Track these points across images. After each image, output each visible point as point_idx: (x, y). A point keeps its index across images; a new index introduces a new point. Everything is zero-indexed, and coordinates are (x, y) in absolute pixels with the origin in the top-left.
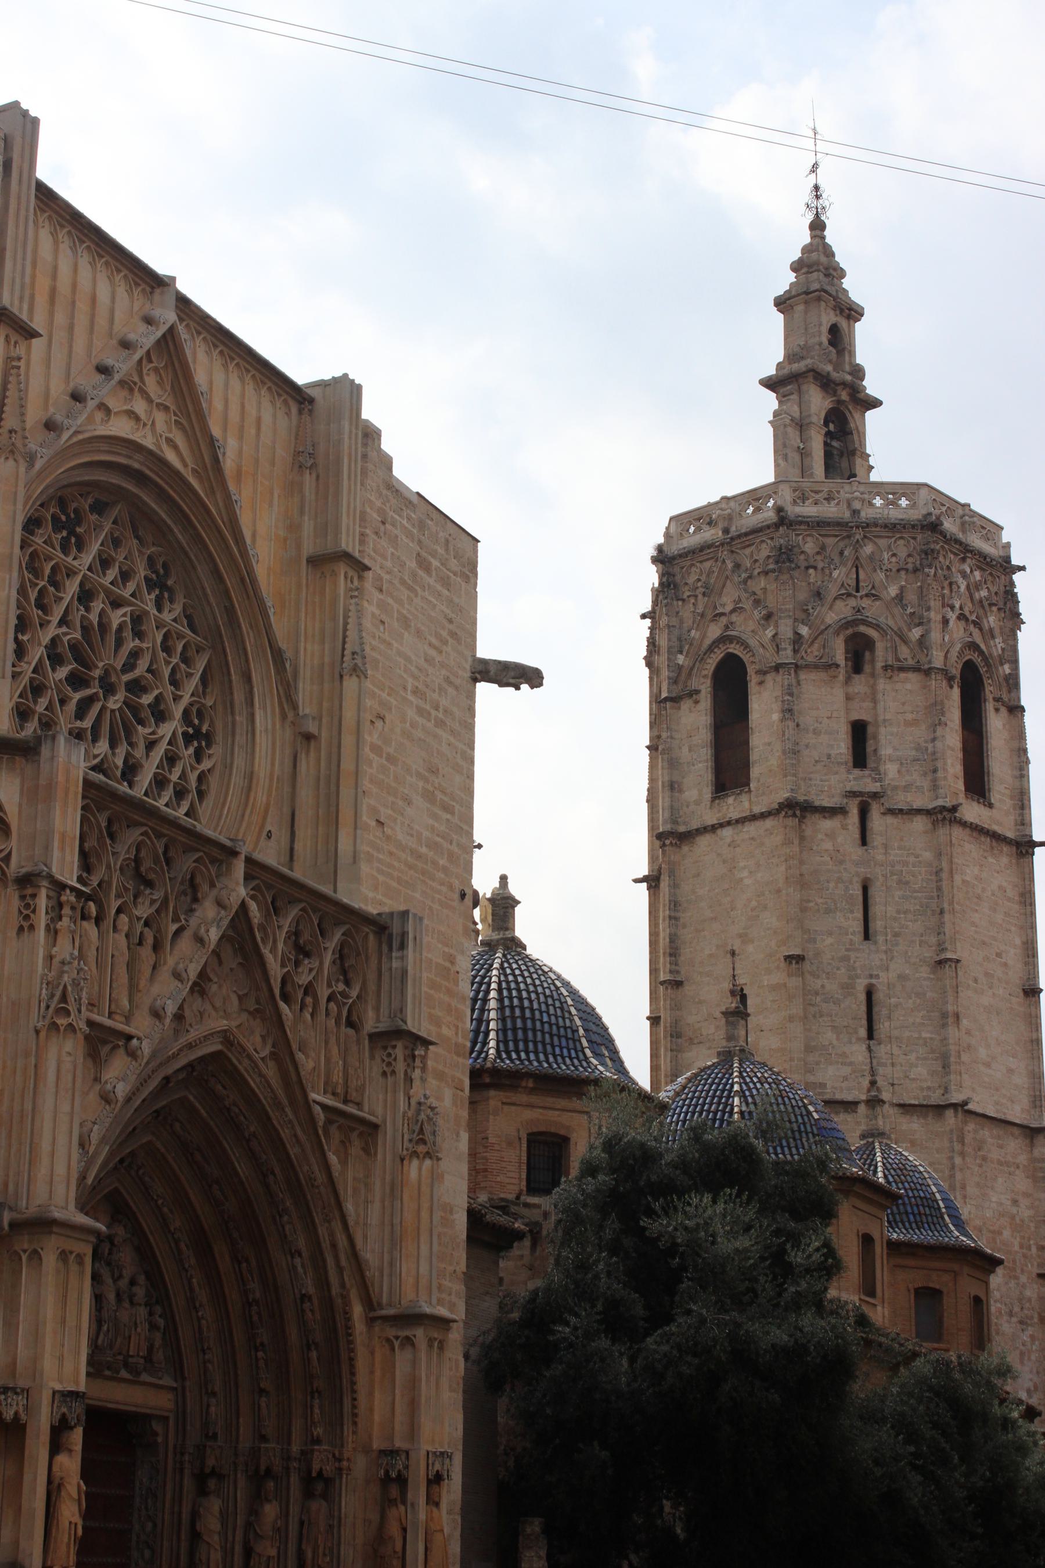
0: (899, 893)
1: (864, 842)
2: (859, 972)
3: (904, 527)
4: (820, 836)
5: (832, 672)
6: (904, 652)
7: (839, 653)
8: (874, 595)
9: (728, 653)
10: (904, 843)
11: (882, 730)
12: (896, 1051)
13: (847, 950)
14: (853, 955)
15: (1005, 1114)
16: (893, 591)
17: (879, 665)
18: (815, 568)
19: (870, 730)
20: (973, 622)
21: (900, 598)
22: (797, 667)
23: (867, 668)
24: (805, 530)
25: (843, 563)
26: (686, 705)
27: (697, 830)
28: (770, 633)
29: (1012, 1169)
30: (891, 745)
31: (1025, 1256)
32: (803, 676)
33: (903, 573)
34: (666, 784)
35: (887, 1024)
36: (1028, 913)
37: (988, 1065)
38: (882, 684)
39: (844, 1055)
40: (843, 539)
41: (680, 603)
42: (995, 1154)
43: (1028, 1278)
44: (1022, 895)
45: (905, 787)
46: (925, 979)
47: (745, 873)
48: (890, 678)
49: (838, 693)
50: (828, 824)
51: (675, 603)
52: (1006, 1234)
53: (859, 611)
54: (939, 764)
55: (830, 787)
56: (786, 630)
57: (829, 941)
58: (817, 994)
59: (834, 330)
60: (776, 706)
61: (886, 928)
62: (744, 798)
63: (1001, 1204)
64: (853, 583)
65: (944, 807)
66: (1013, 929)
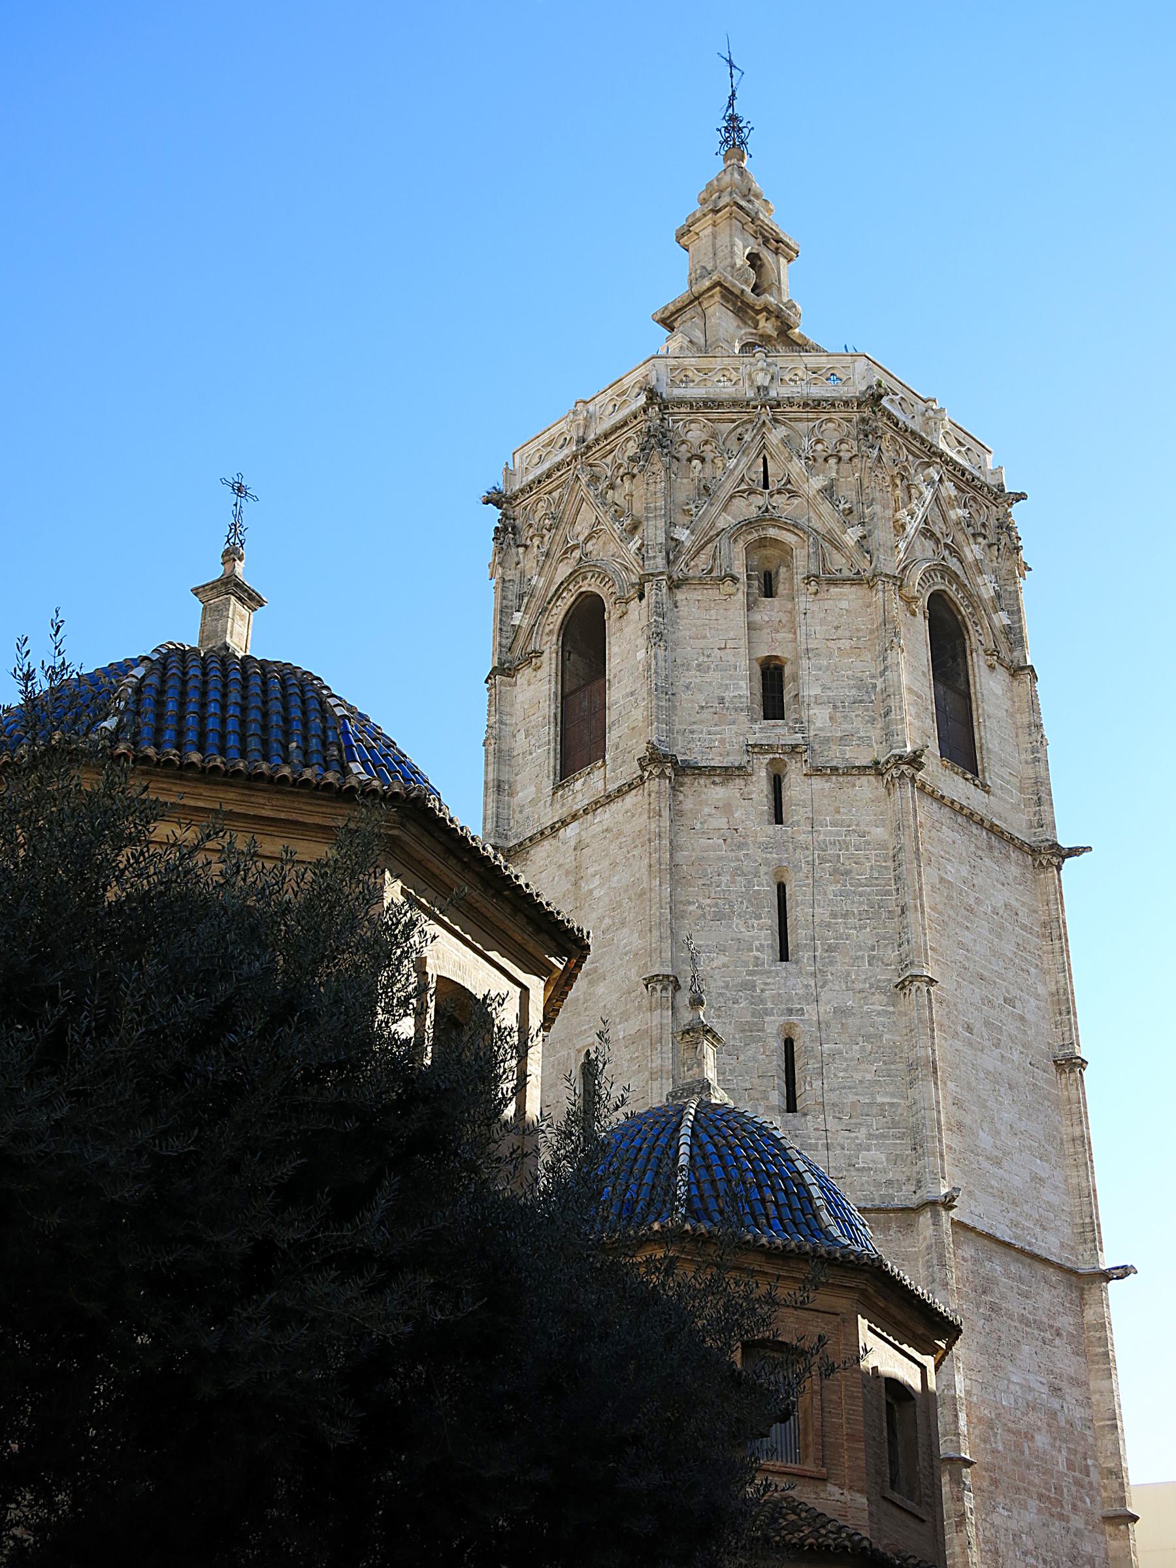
1: (779, 819)
3: (833, 405)
4: (706, 810)
5: (728, 587)
6: (838, 561)
9: (582, 593)
10: (843, 817)
11: (804, 663)
12: (832, 1124)
14: (759, 980)
15: (1030, 1244)
16: (817, 482)
17: (798, 579)
18: (703, 460)
19: (787, 671)
20: (946, 546)
21: (829, 491)
22: (675, 585)
23: (782, 588)
25: (744, 452)
27: (531, 839)
28: (634, 545)
29: (1048, 1335)
31: (1078, 1483)
32: (680, 595)
33: (832, 461)
34: (491, 785)
35: (817, 1084)
36: (1057, 949)
37: (998, 1163)
41: (521, 550)
42: (1013, 1304)
43: (1087, 1523)
44: (1044, 925)
45: (841, 738)
46: (879, 1014)
47: (597, 881)
48: (816, 593)
50: (718, 793)
51: (514, 550)
52: (1042, 1440)
53: (767, 510)
54: (892, 703)
56: (654, 531)
57: (722, 959)
59: (754, 259)
60: (642, 641)
62: (598, 774)
63: (1031, 1389)
65: (901, 757)
66: (1033, 970)
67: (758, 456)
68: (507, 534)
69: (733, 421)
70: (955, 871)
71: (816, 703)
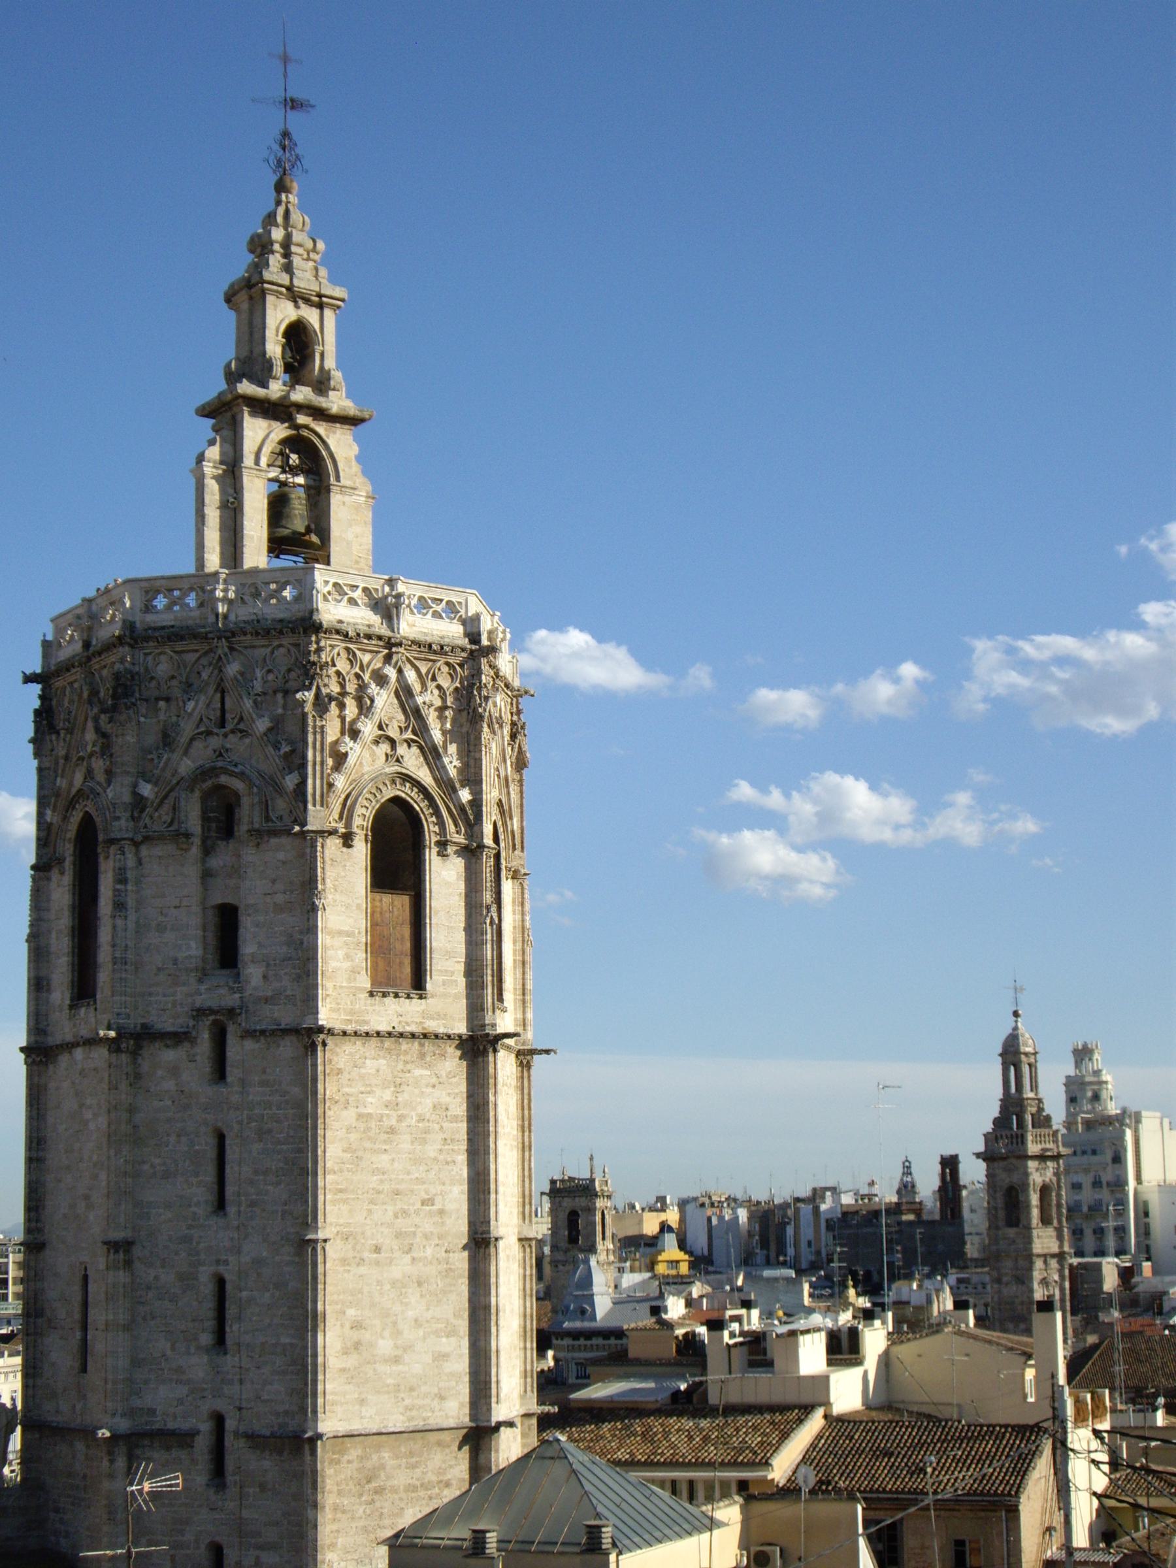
0: (256, 1147)
2: (203, 1257)
3: (281, 632)
8: (241, 731)
13: (190, 1227)
16: (262, 725)
18: (167, 700)
24: (156, 647)
26: (55, 874)
32: (144, 851)
39: (179, 1370)
40: (206, 653)
41: (54, 737)
49: (192, 872)
50: (170, 1056)
51: (48, 738)
53: (221, 755)
55: (174, 1004)
57: (169, 1215)
58: (149, 1288)
61: (239, 1195)
64: (215, 715)
67: (216, 691)
68: (45, 718)
69: (197, 651)
71: (253, 961)
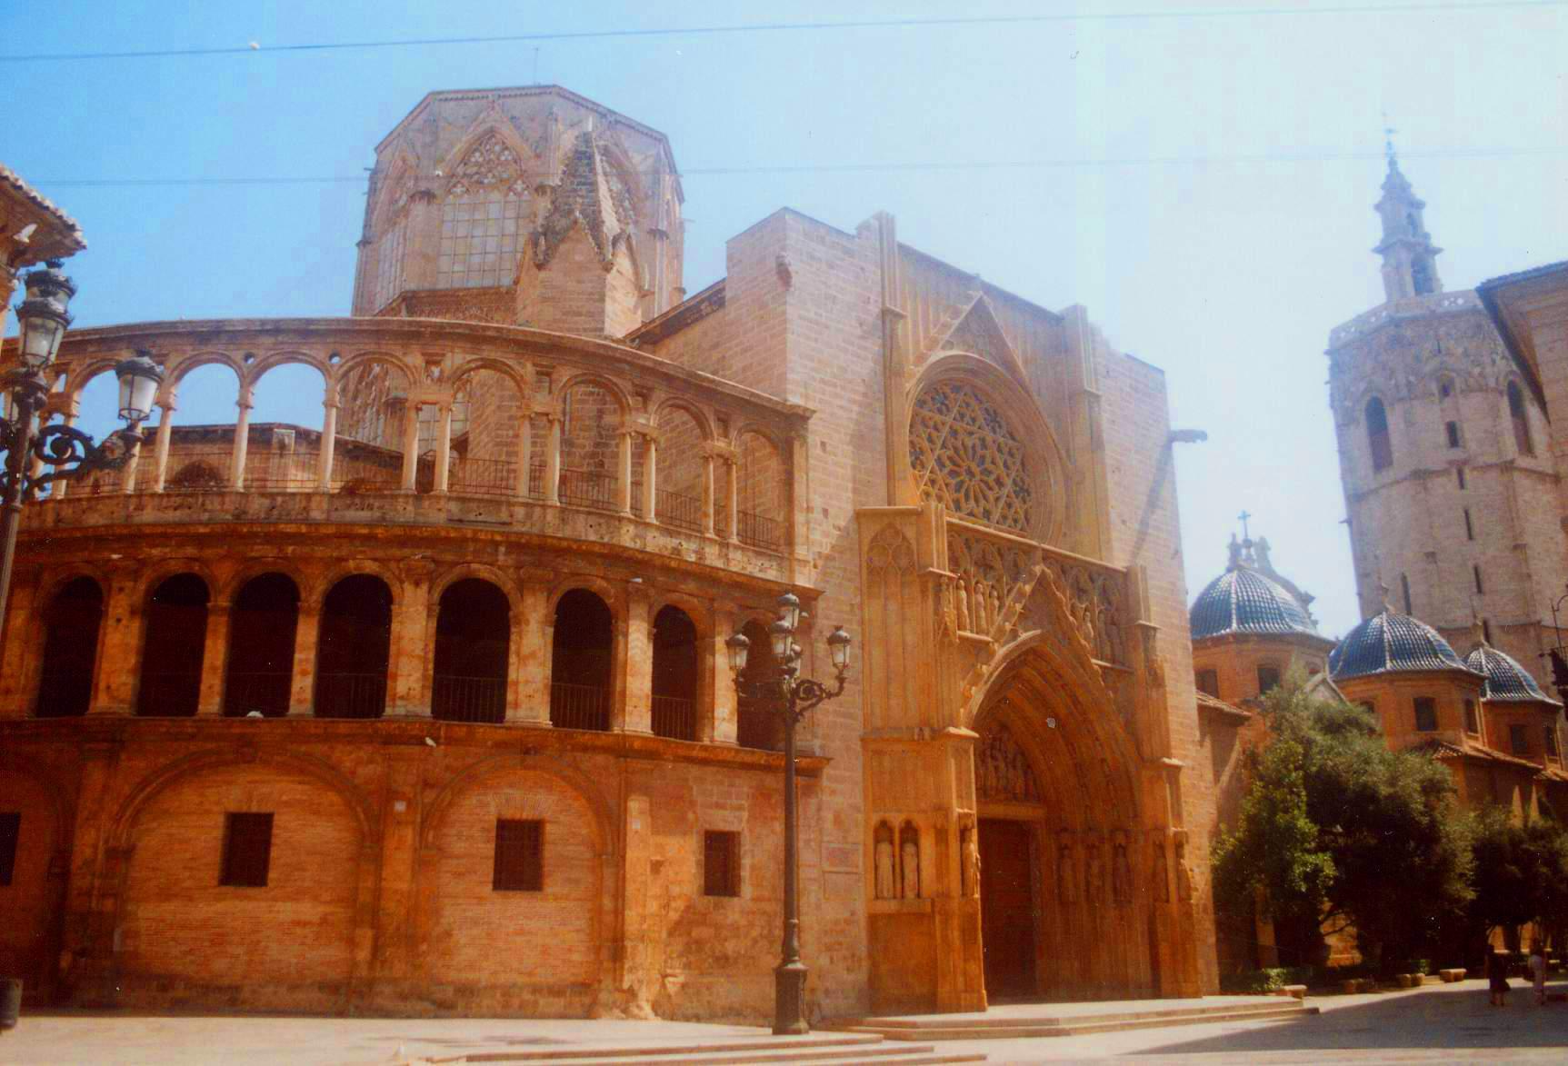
1: (1462, 486)
7: (1434, 387)
16: (1460, 350)
21: (1466, 354)
30: (1469, 433)
38: (1461, 400)
56: (1401, 379)
59: (1410, 216)
70: (1527, 496)
